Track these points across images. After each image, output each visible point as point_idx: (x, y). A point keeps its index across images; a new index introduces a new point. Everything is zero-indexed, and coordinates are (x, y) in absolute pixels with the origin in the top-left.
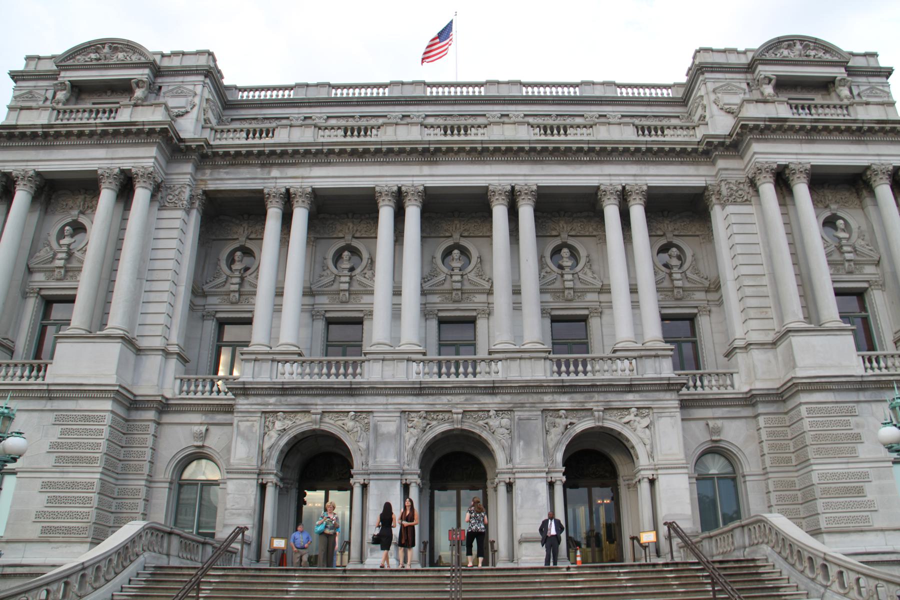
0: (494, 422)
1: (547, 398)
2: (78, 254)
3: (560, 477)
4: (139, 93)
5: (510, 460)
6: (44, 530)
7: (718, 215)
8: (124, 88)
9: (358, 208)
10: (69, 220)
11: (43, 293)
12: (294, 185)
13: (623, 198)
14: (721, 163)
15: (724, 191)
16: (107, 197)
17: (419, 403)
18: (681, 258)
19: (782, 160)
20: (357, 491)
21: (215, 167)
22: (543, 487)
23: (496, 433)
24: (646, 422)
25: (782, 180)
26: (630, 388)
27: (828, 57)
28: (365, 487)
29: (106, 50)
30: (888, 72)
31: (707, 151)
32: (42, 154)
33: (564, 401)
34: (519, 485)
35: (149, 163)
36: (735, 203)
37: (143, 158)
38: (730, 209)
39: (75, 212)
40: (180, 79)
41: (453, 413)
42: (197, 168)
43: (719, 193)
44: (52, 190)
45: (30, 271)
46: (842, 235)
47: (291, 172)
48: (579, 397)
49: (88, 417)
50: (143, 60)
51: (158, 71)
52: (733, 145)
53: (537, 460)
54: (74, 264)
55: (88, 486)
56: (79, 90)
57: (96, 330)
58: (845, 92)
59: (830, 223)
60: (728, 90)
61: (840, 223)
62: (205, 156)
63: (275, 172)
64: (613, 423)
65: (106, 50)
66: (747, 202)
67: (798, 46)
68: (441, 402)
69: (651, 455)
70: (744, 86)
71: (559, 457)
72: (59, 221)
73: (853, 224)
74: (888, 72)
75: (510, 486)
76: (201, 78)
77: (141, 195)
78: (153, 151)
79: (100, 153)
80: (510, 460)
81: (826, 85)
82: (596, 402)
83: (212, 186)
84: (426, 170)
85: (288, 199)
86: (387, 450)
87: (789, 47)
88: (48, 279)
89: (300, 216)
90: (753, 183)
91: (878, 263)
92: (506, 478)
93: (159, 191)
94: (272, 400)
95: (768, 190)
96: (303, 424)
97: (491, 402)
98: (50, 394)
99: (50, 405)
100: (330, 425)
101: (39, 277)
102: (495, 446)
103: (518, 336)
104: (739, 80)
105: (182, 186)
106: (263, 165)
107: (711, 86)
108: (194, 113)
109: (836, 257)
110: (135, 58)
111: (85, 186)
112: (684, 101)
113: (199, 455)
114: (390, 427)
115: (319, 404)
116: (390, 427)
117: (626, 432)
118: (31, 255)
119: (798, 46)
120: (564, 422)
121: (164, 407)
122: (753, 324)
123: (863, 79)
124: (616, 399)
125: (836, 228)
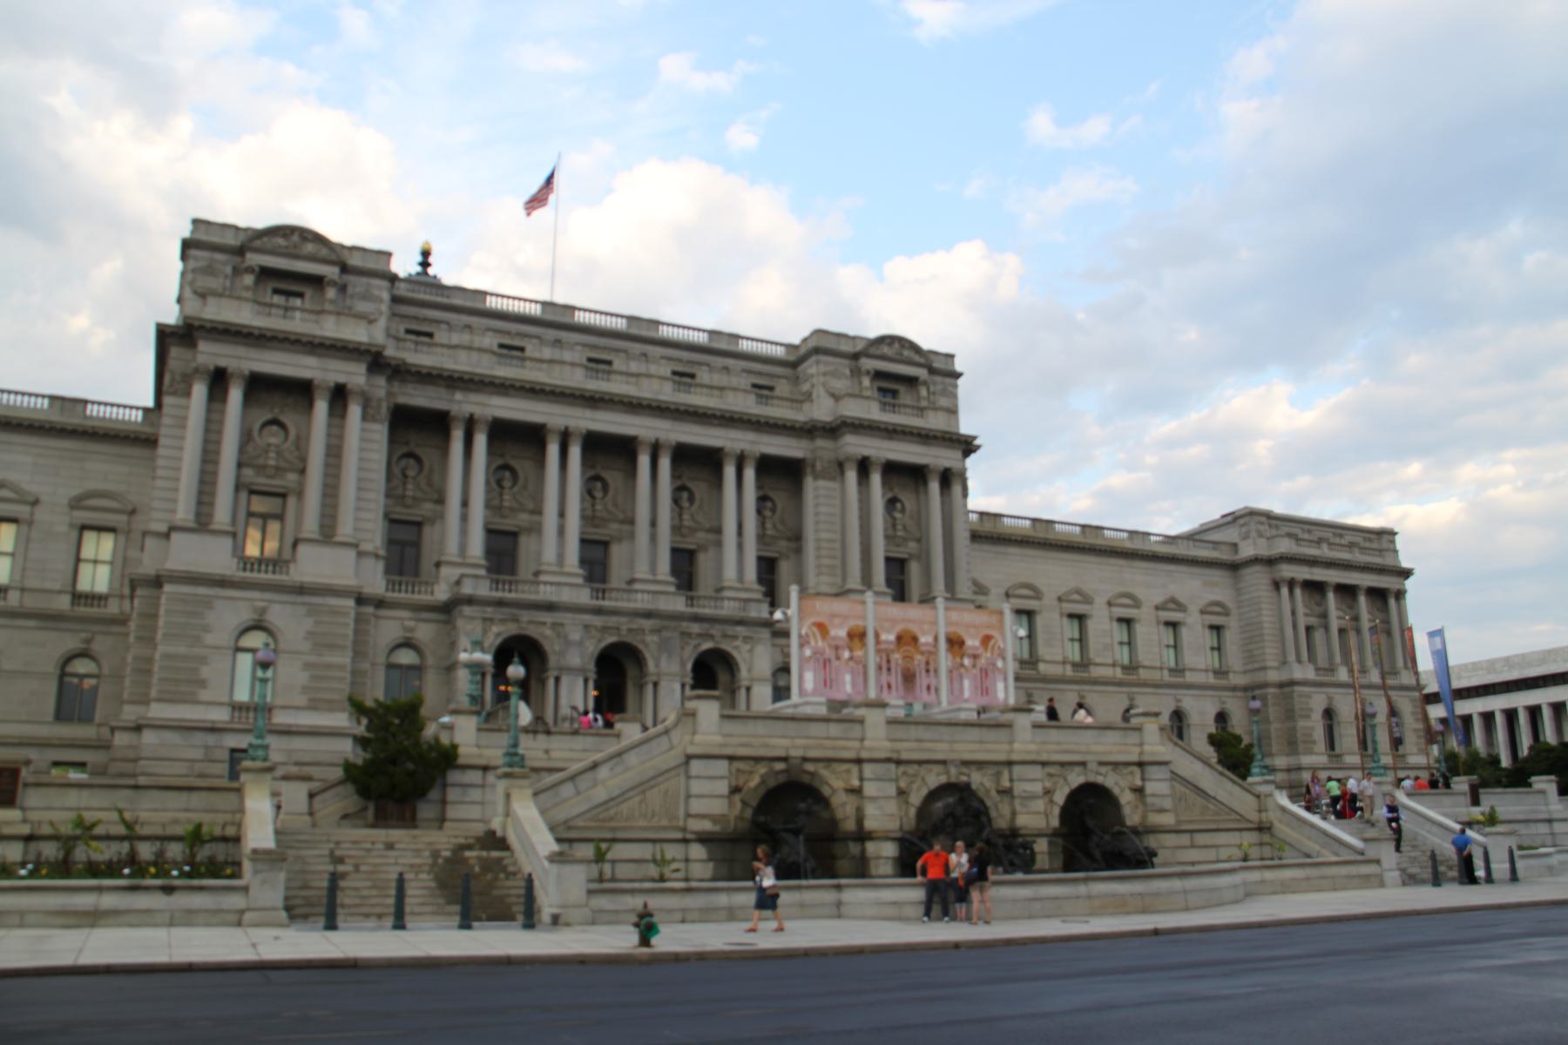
1: (684, 624)
3: (689, 680)
4: (331, 293)
5: (657, 666)
6: (310, 700)
7: (811, 486)
9: (531, 437)
12: (478, 411)
14: (820, 443)
15: (819, 466)
16: (321, 407)
17: (597, 621)
18: (773, 510)
19: (866, 452)
20: (551, 683)
21: (403, 381)
22: (677, 687)
23: (649, 645)
24: (747, 647)
25: (864, 466)
26: (740, 622)
27: (917, 358)
28: (557, 680)
29: (296, 238)
30: (958, 375)
31: (809, 431)
32: (253, 353)
33: (695, 628)
34: (663, 684)
36: (824, 478)
37: (354, 374)
38: (821, 483)
40: (364, 280)
41: (623, 630)
42: (390, 379)
43: (813, 466)
46: (898, 515)
47: (474, 397)
48: (706, 626)
49: (334, 612)
50: (333, 257)
51: (345, 268)
52: (833, 430)
53: (675, 667)
55: (342, 667)
57: (327, 535)
58: (924, 392)
59: (891, 503)
60: (835, 374)
61: (898, 505)
62: (399, 372)
63: (458, 396)
64: (726, 646)
65: (296, 238)
66: (833, 479)
67: (897, 345)
68: (613, 621)
69: (749, 671)
70: (847, 372)
71: (689, 666)
73: (908, 506)
74: (958, 375)
75: (656, 685)
77: (355, 411)
79: (311, 361)
80: (657, 666)
81: (911, 381)
82: (716, 630)
83: (402, 400)
84: (588, 413)
85: (470, 425)
86: (574, 653)
87: (890, 344)
89: (481, 441)
90: (841, 466)
91: (919, 540)
92: (654, 678)
93: (367, 403)
94: (489, 609)
95: (852, 476)
96: (511, 629)
97: (647, 624)
98: (301, 590)
99: (300, 599)
100: (532, 631)
102: (647, 655)
103: (653, 570)
104: (844, 366)
105: (379, 400)
106: (448, 387)
107: (822, 368)
109: (890, 532)
110: (324, 252)
111: (302, 390)
112: (794, 365)
113: (407, 644)
114: (575, 636)
115: (526, 616)
116: (575, 636)
117: (735, 653)
119: (897, 345)
120: (694, 642)
121: (380, 603)
122: (824, 579)
123: (938, 379)
124: (730, 630)
125: (894, 509)
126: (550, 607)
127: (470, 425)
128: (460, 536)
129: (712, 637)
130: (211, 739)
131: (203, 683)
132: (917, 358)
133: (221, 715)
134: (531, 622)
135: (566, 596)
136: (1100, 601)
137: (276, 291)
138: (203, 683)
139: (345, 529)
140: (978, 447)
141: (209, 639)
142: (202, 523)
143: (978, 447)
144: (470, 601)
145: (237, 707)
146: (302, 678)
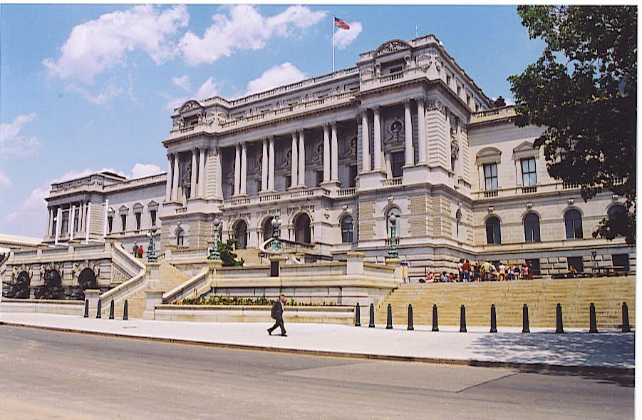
2: (401, 135)
8: (403, 61)
10: (394, 121)
11: (392, 151)
35: (421, 94)
39: (396, 118)
44: (386, 112)
45: (385, 144)
51: (413, 50)
54: (400, 139)
56: (384, 66)
72: (390, 123)
76: (431, 49)
77: (421, 110)
78: (421, 89)
88: (392, 146)
98: (404, 189)
101: (389, 146)
108: (433, 66)
118: (385, 139)
137: (392, 71)
142: (373, 172)
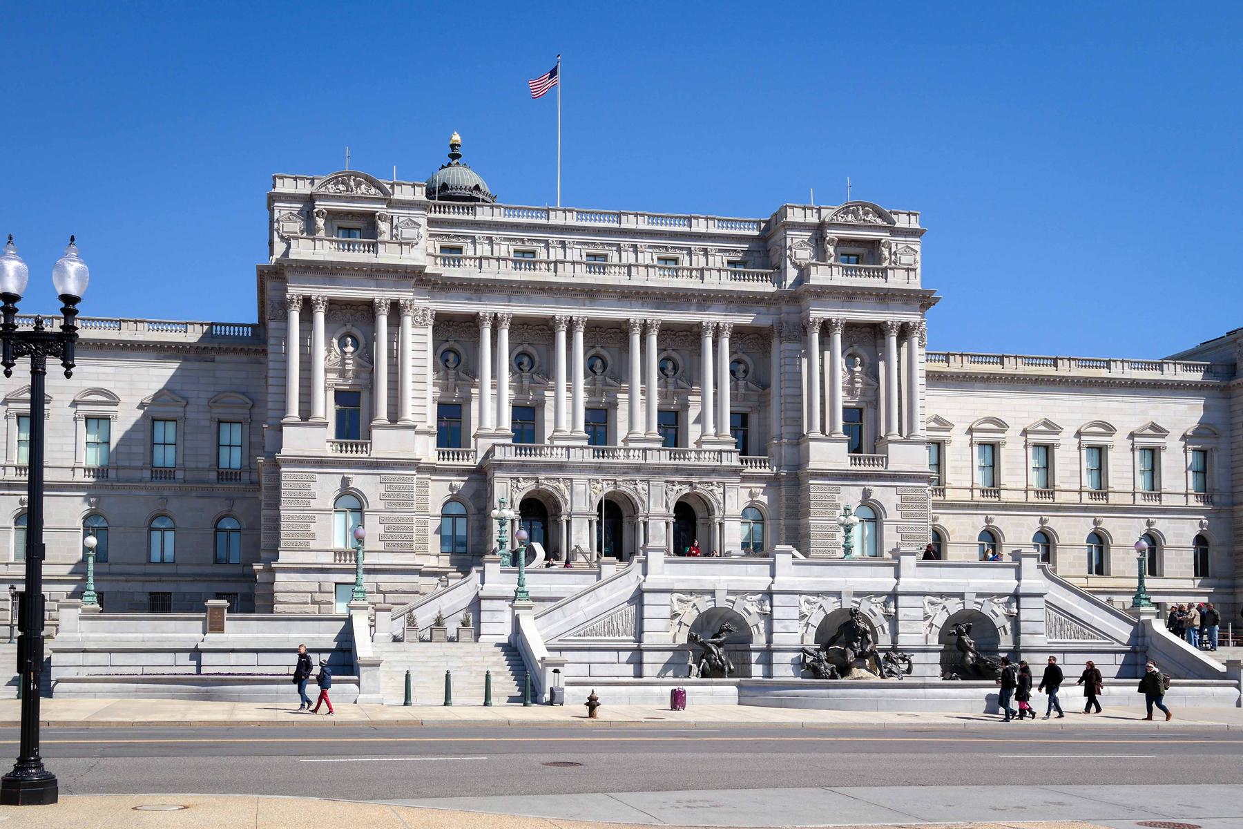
0: (639, 486)
13: (717, 332)
22: (663, 524)
28: (568, 522)
36: (789, 340)
50: (382, 196)
71: (672, 506)
77: (408, 321)
86: (581, 500)
89: (505, 335)
120: (677, 488)
126: (560, 467)
127: (496, 322)
128: (491, 410)
129: (691, 484)
130: (321, 577)
131: (312, 537)
132: (879, 222)
133: (327, 559)
134: (546, 479)
135: (576, 457)
136: (1069, 431)
138: (312, 537)
139: (410, 413)
140: (937, 299)
141: (314, 504)
143: (937, 299)
144: (501, 465)
145: (337, 553)
146: (380, 529)
